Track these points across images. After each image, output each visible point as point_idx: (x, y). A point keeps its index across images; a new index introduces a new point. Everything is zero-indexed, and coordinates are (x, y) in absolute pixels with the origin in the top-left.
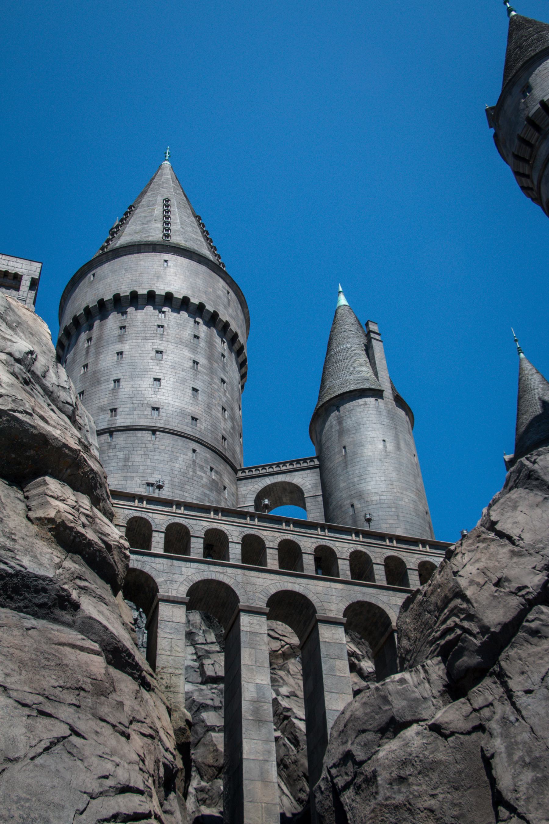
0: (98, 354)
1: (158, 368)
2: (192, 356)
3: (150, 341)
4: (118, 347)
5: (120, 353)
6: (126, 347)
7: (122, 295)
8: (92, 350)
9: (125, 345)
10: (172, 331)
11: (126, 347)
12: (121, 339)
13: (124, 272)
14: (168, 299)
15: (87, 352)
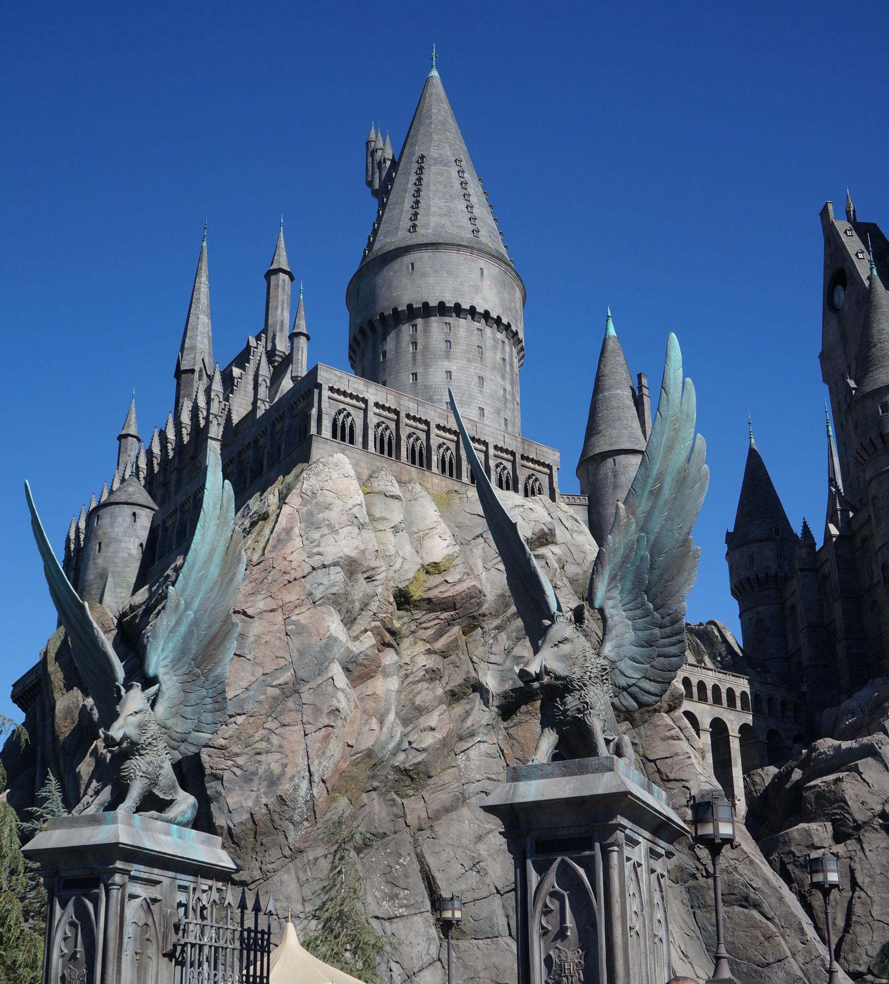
0: (426, 366)
1: (481, 396)
2: (503, 383)
3: (473, 364)
4: (446, 365)
5: (449, 373)
6: (453, 366)
7: (447, 305)
8: (419, 358)
9: (452, 364)
10: (488, 355)
11: (453, 366)
12: (448, 355)
13: (445, 275)
14: (486, 315)
15: (414, 359)
